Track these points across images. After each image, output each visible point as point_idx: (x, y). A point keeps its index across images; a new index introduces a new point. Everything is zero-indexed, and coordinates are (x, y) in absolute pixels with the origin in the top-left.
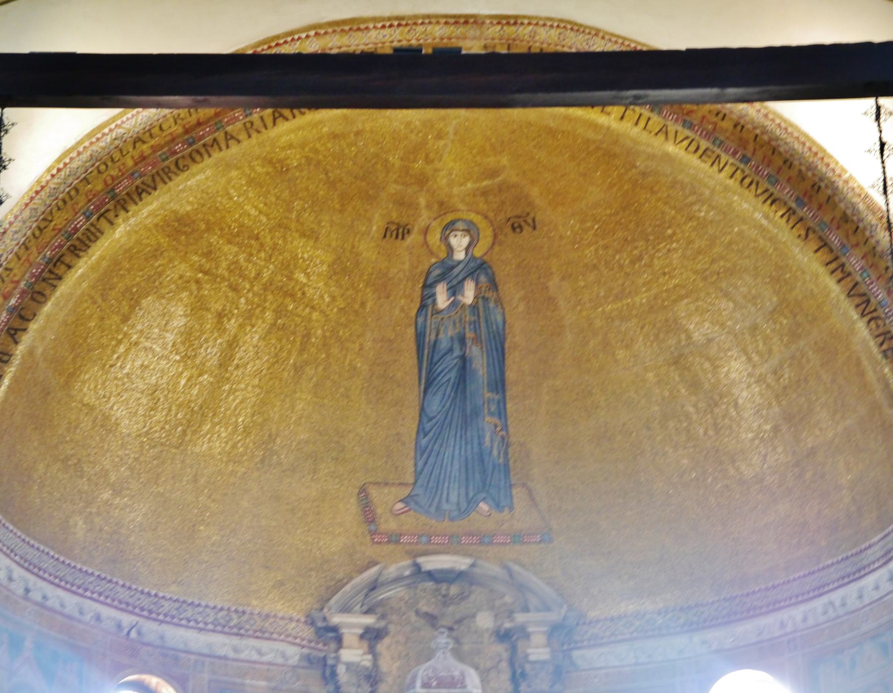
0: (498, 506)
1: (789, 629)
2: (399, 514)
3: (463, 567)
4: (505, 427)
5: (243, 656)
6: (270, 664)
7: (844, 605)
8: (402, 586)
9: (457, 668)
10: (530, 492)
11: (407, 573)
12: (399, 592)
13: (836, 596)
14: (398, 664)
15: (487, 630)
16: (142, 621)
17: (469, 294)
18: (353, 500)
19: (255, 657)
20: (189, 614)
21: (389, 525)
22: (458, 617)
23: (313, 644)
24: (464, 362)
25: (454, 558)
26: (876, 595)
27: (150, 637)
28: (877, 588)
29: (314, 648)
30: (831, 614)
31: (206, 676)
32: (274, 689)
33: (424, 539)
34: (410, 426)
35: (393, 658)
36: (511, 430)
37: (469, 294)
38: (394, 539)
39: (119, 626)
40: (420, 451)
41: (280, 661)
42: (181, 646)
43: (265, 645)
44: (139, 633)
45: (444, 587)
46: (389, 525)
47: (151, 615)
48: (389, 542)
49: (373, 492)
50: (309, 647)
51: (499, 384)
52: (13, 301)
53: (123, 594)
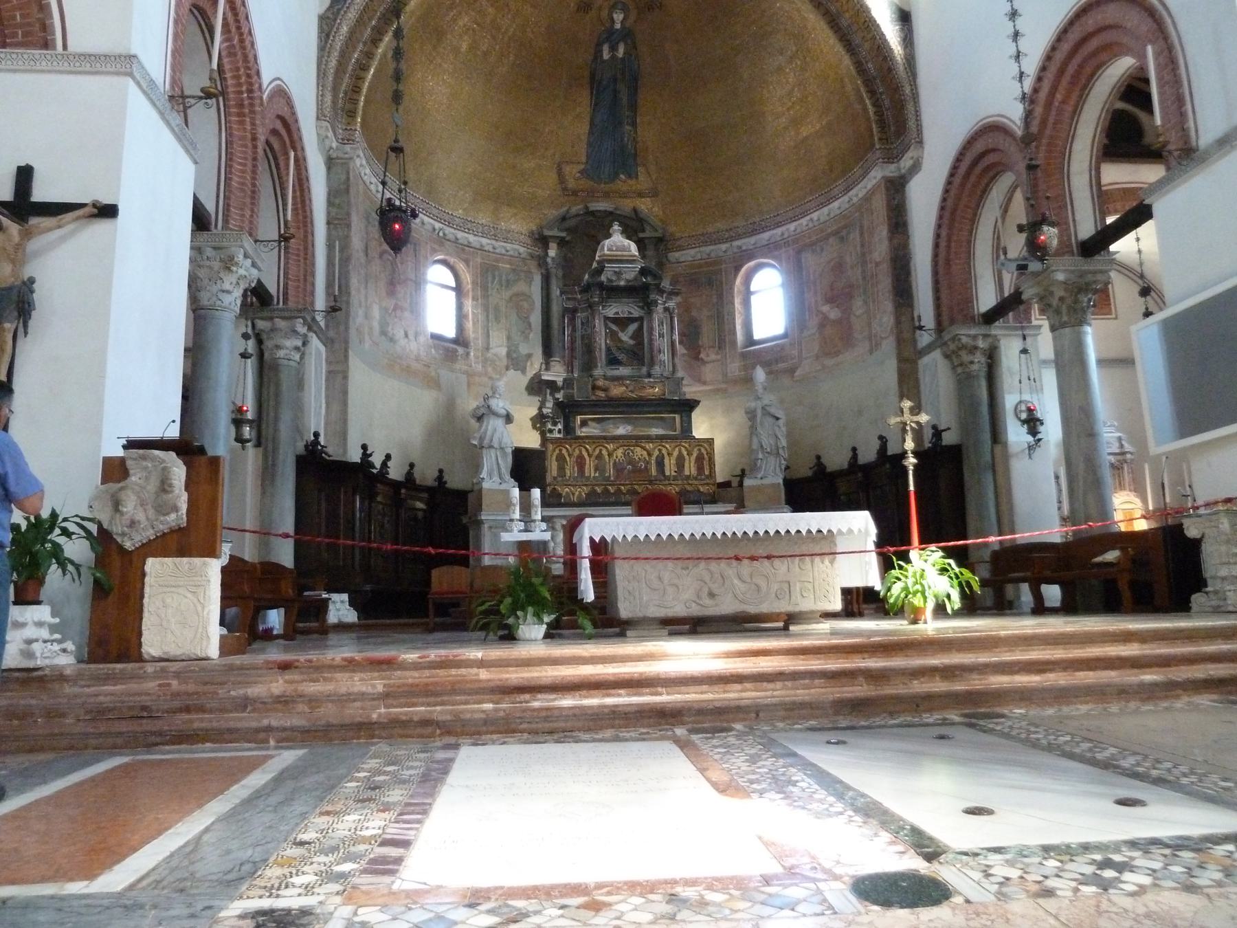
0: (630, 177)
1: (786, 236)
4: (636, 132)
5: (497, 251)
6: (511, 256)
7: (819, 219)
9: (627, 242)
10: (647, 170)
13: (815, 216)
16: (445, 227)
17: (621, 52)
19: (504, 252)
20: (469, 226)
21: (571, 184)
24: (615, 92)
26: (838, 212)
27: (450, 237)
28: (839, 208)
30: (811, 225)
31: (479, 260)
32: (514, 270)
34: (584, 128)
36: (639, 133)
37: (621, 52)
38: (575, 193)
39: (434, 229)
40: (590, 145)
41: (516, 255)
42: (466, 243)
43: (509, 246)
44: (444, 234)
46: (571, 184)
47: (449, 225)
49: (563, 166)
51: (633, 107)
52: (374, 23)
53: (435, 212)
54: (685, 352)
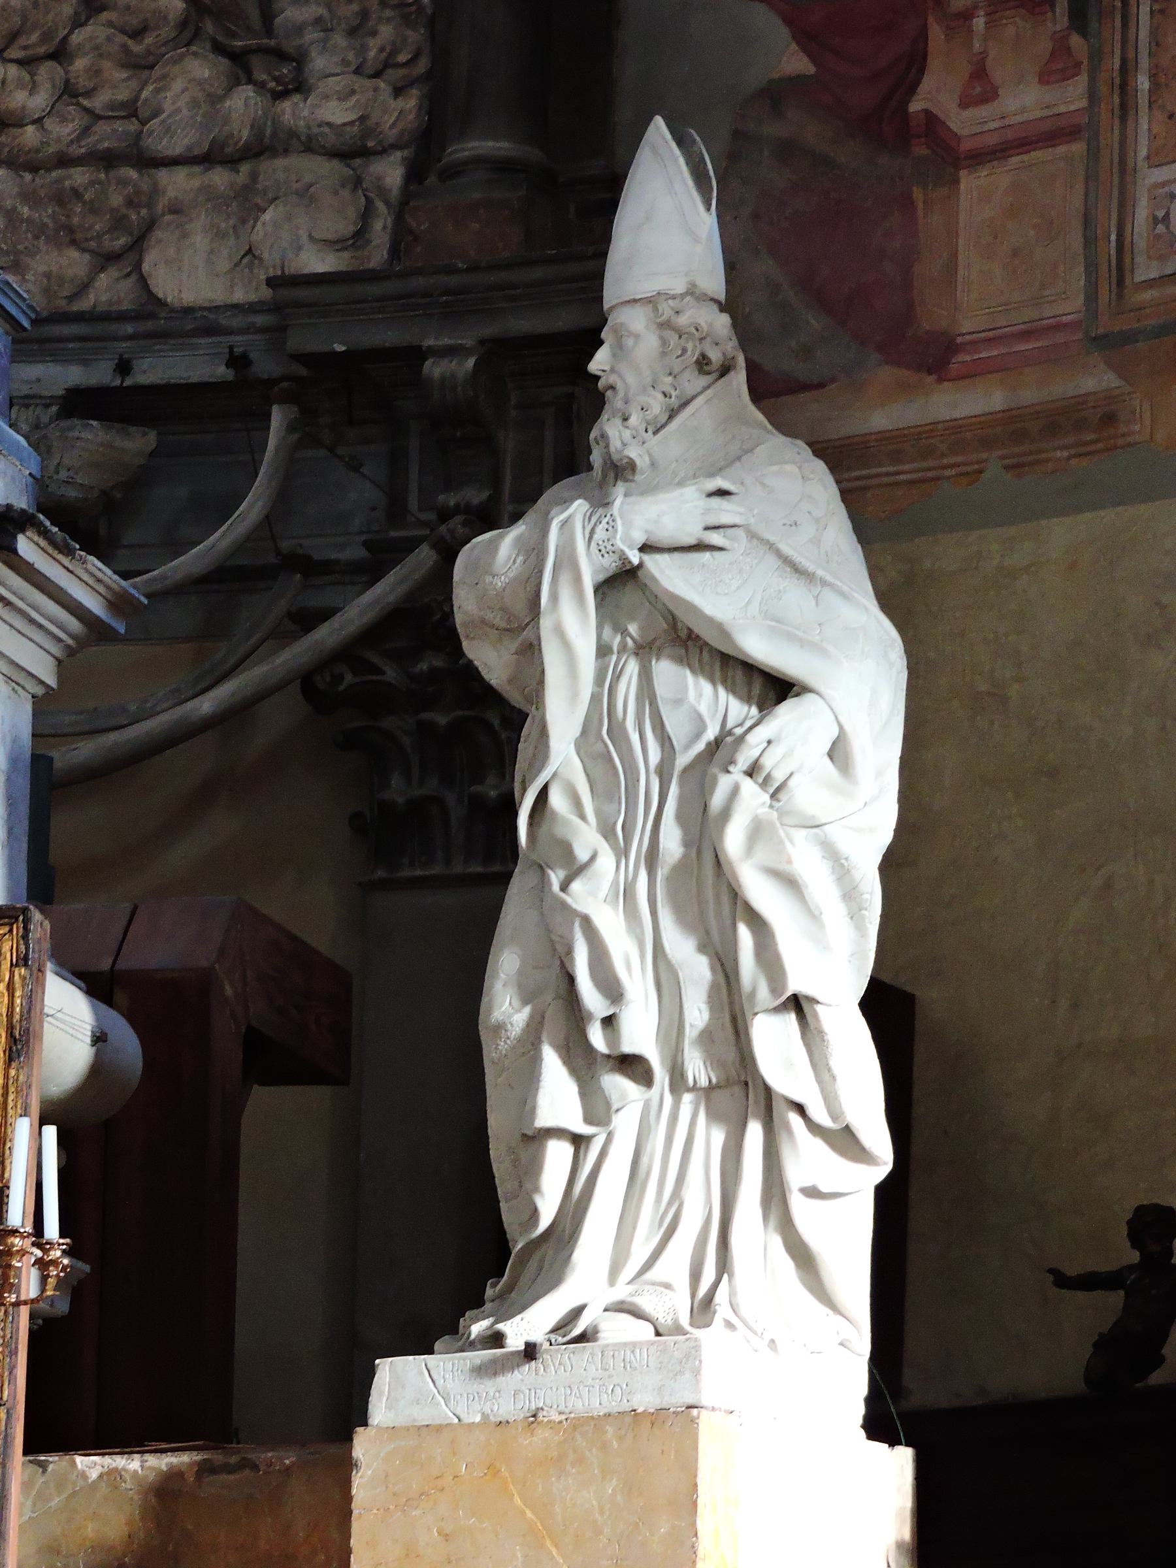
54: (796, 63)
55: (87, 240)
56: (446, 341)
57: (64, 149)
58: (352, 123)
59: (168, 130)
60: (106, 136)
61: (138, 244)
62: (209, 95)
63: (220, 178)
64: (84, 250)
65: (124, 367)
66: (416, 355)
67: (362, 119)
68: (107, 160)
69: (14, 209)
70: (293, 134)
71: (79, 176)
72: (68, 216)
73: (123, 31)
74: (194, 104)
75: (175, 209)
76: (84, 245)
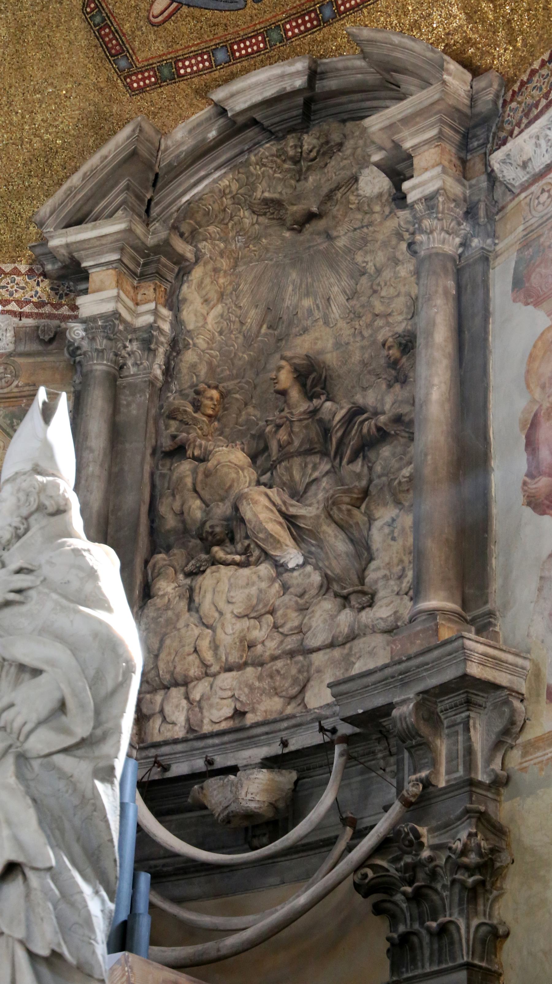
2: (164, 21)
3: (299, 82)
8: (217, 169)
11: (212, 134)
12: (215, 181)
14: (219, 308)
15: (380, 195)
18: (76, 23)
22: (325, 190)
23: (47, 309)
25: (276, 70)
29: (50, 316)
33: (221, 56)
35: (206, 301)
45: (291, 141)
48: (160, 82)
50: (39, 316)
55: (282, 692)
56: (403, 697)
57: (273, 652)
58: (391, 616)
59: (314, 635)
60: (291, 643)
61: (303, 690)
62: (331, 616)
63: (337, 653)
64: (281, 697)
65: (285, 744)
66: (390, 706)
67: (396, 613)
68: (291, 654)
69: (253, 683)
70: (366, 626)
71: (279, 664)
72: (274, 683)
73: (296, 595)
74: (325, 621)
75: (318, 671)
76: (281, 694)
